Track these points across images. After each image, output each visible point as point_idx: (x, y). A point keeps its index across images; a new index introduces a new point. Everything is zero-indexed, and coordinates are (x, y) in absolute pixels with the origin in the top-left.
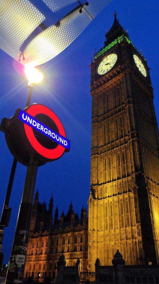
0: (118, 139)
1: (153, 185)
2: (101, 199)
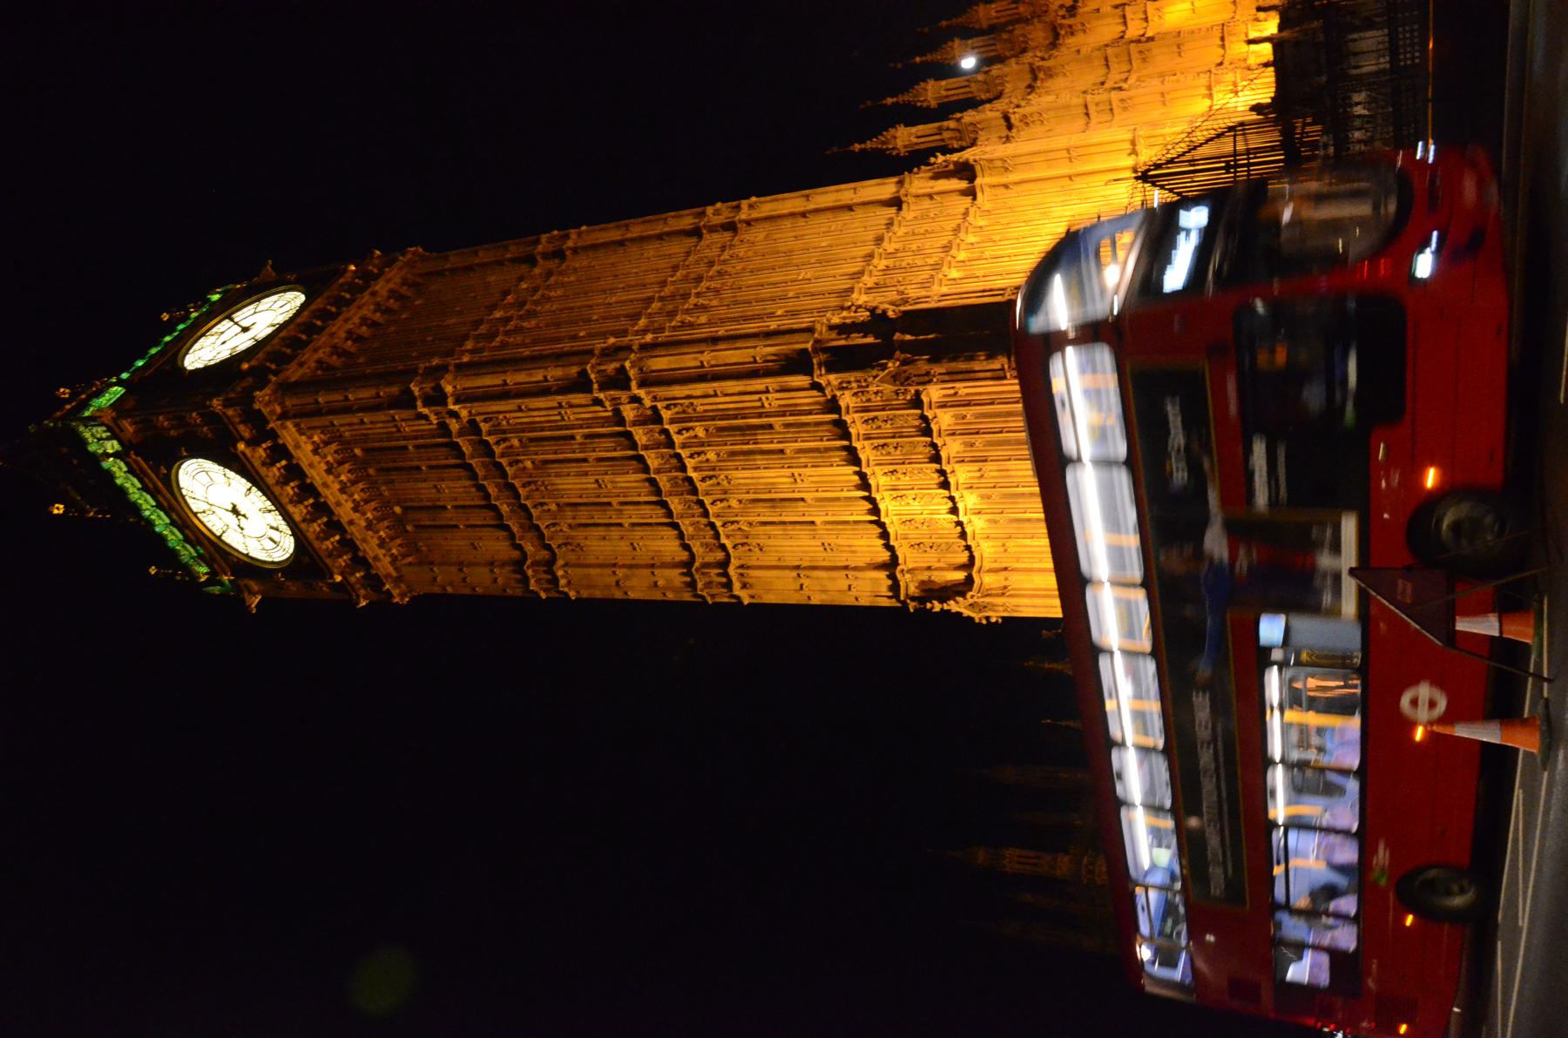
0: (641, 459)
1: (881, 267)
2: (968, 548)
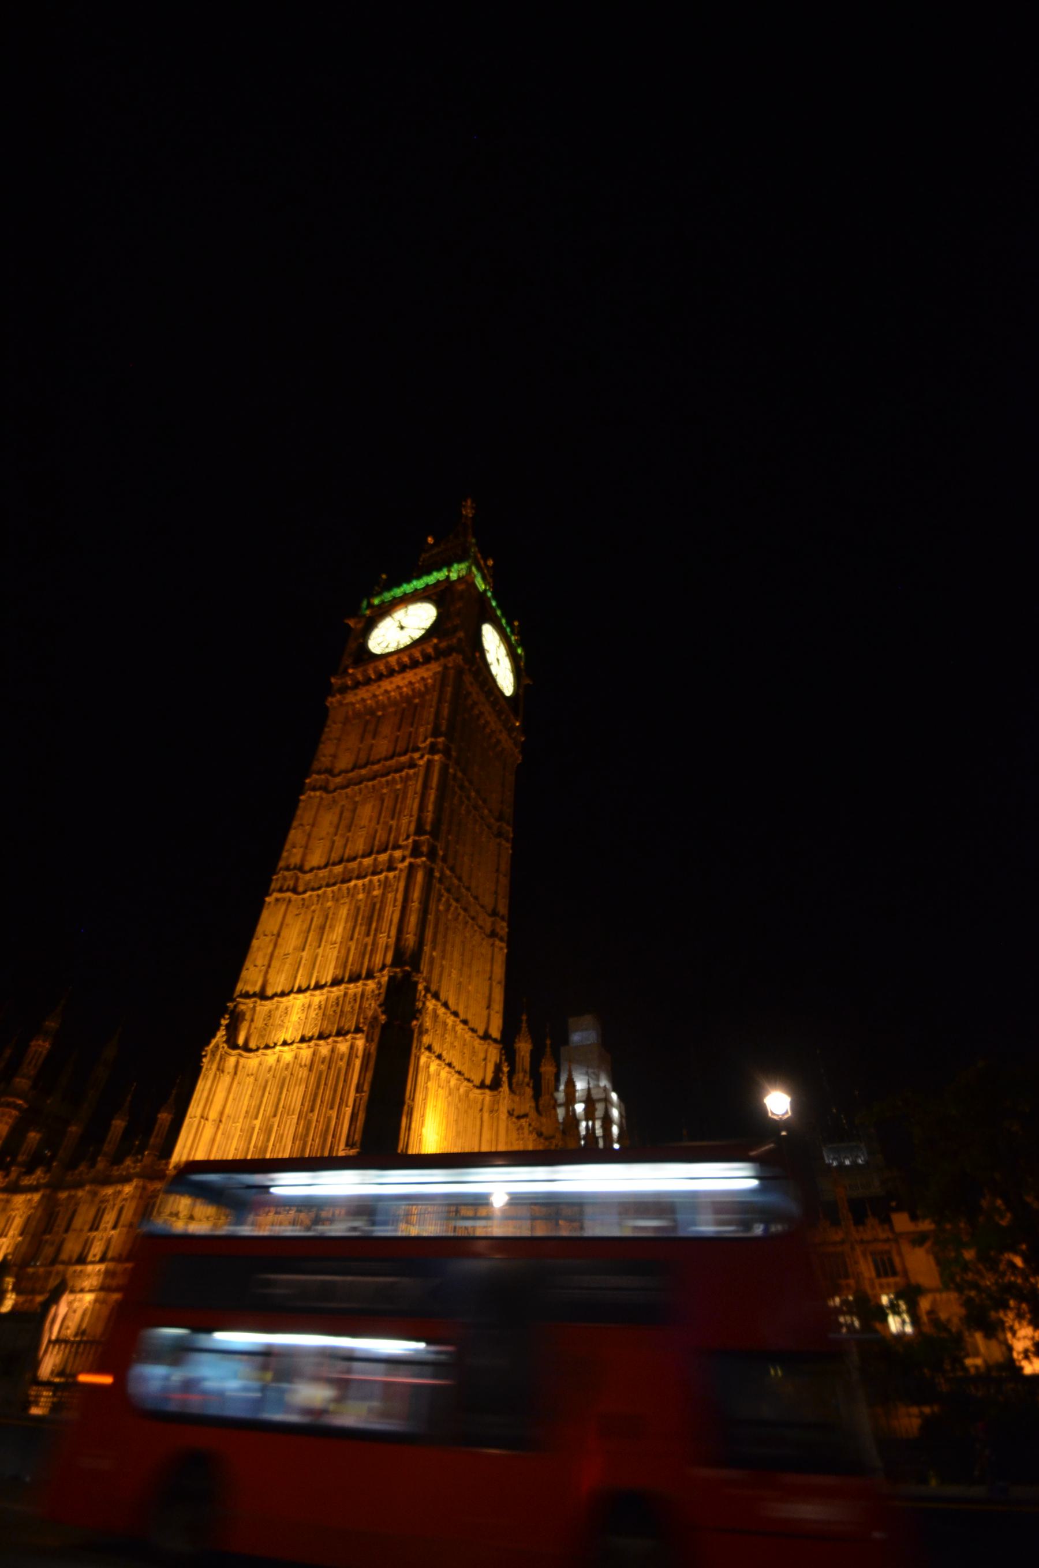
0: (369, 854)
2: (257, 1049)
